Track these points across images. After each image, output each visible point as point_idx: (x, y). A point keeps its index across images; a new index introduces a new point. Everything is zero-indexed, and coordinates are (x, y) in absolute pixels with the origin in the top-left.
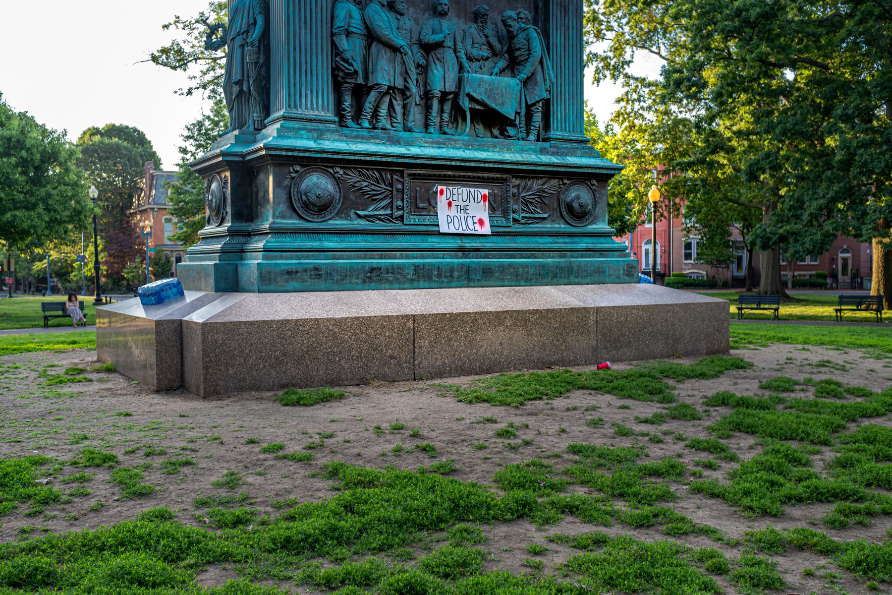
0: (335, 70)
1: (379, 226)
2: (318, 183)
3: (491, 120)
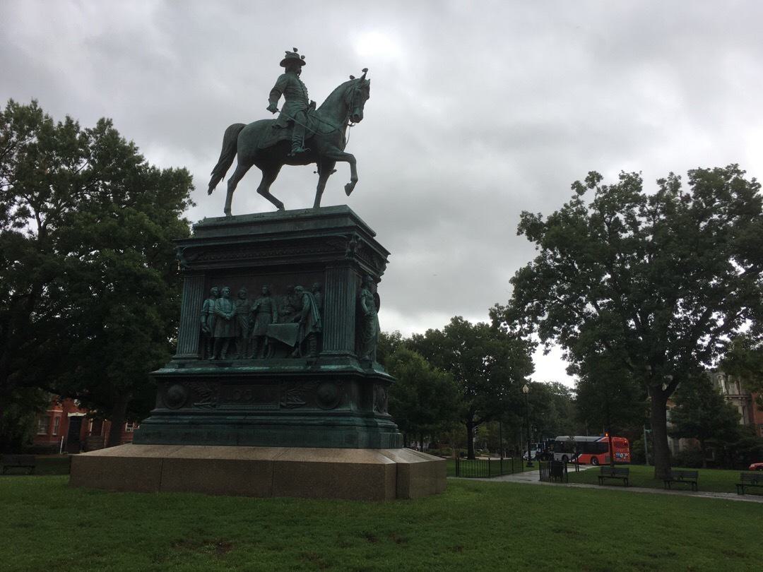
0: (202, 334)
1: (202, 410)
3: (279, 348)
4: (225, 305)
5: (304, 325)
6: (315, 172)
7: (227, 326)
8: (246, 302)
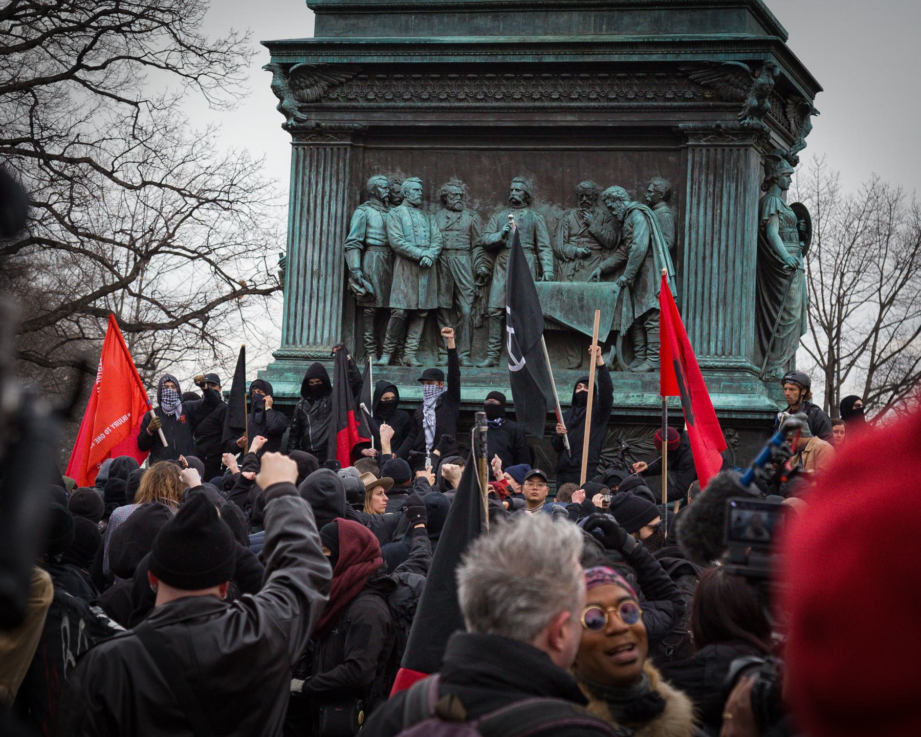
0: (348, 293)
4: (414, 226)
5: (635, 287)
7: (423, 281)
8: (467, 219)
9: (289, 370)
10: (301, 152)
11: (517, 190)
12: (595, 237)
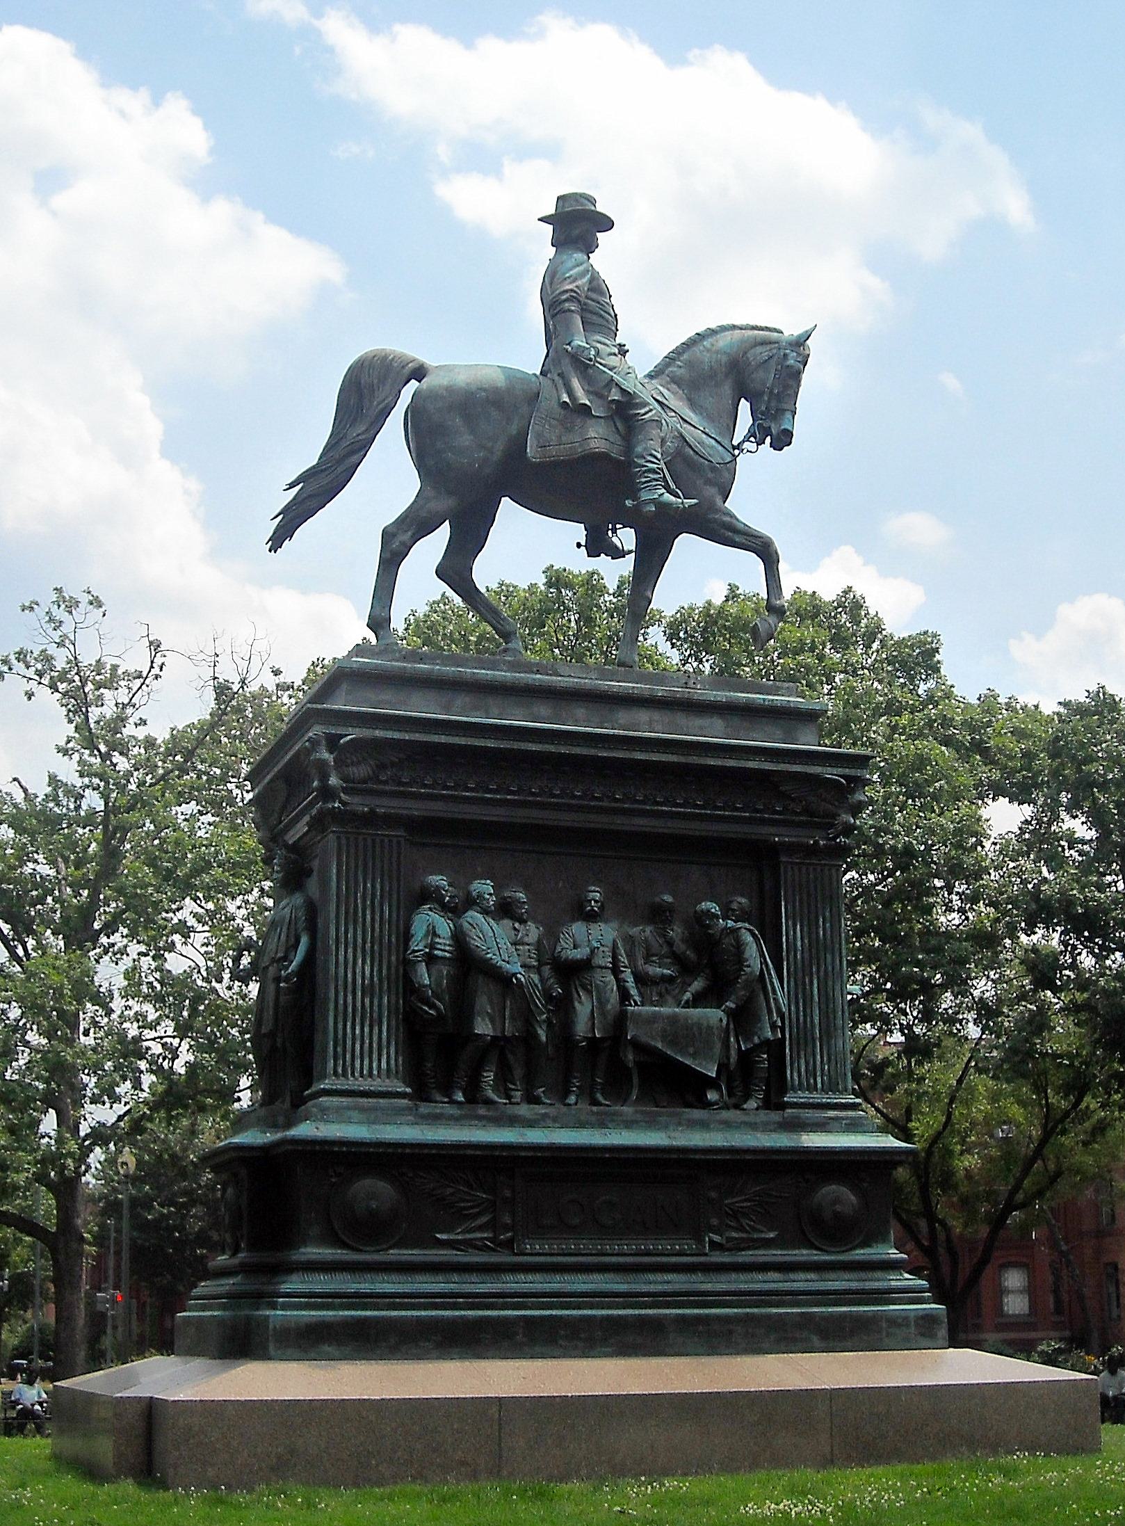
2: (374, 1192)
6: (579, 545)
9: (348, 1108)
10: (344, 841)
11: (596, 901)
12: (678, 959)
